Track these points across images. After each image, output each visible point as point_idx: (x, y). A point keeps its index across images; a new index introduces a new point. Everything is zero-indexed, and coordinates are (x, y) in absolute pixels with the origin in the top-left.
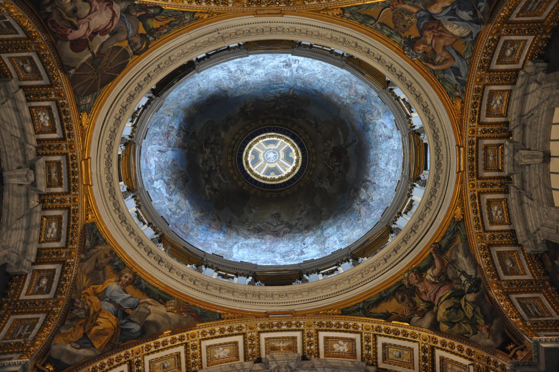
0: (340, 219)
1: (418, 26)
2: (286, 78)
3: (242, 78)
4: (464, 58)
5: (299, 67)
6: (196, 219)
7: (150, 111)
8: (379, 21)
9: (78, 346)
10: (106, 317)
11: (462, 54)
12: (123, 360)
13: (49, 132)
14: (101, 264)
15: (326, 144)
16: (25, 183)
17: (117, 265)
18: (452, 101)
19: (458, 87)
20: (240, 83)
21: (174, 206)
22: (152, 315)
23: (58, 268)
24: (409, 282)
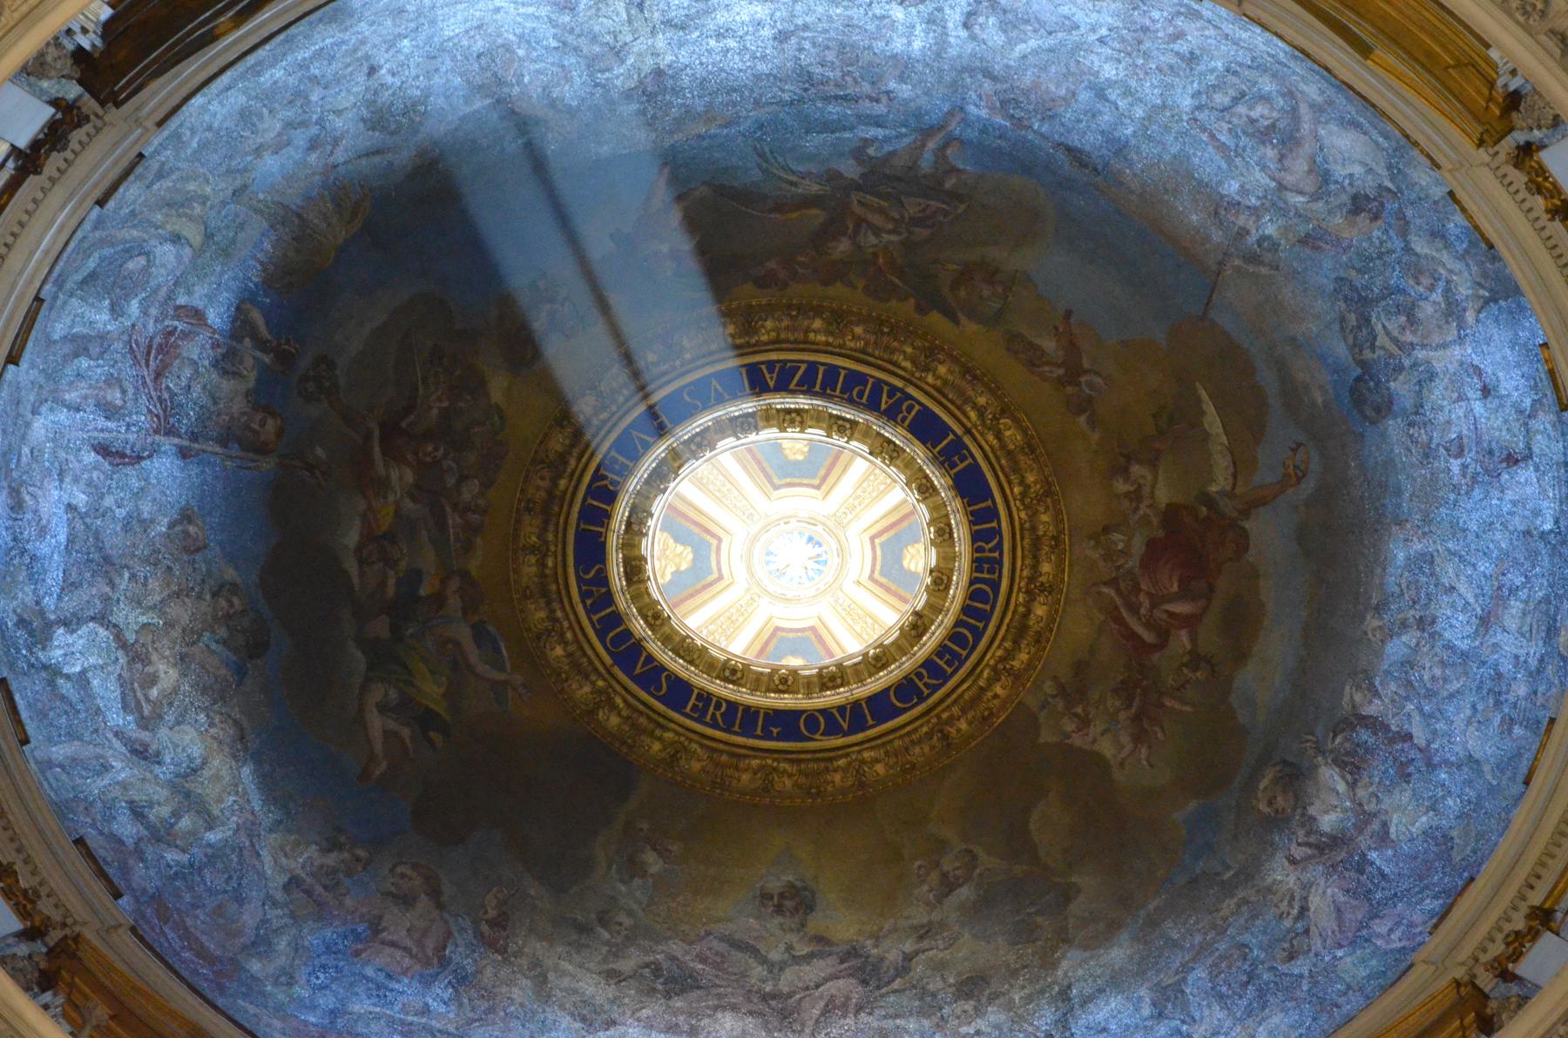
0: (1175, 944)
2: (904, 66)
6: (293, 883)
7: (58, 194)
15: (1121, 487)
21: (164, 793)
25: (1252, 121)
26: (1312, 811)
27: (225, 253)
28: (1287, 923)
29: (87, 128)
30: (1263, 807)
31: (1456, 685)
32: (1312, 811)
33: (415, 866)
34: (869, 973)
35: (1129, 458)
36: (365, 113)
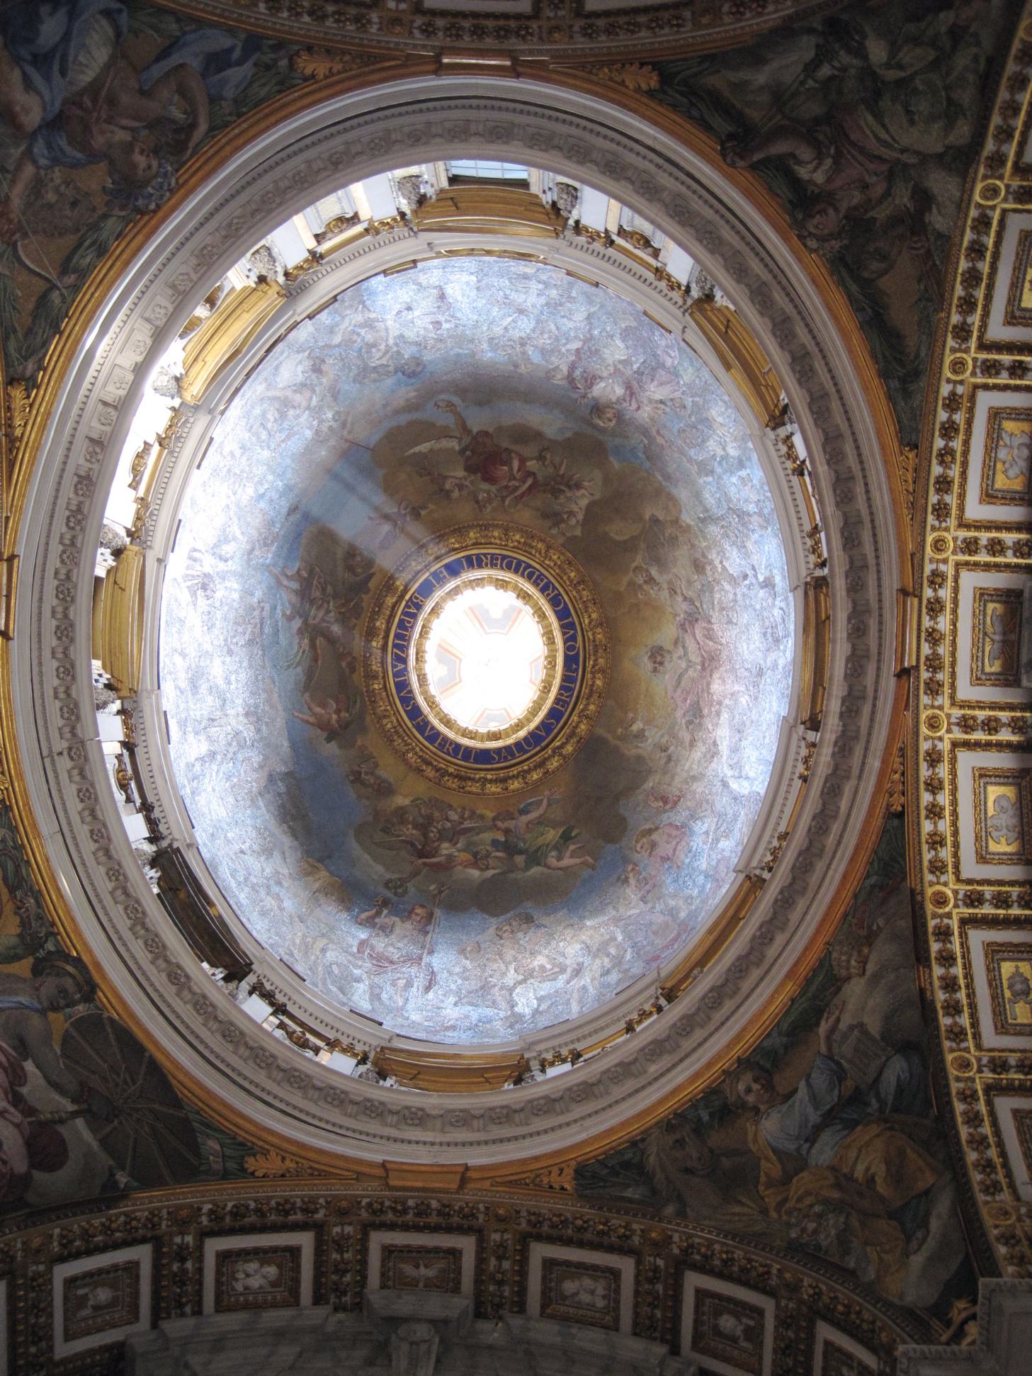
1: (75, 165)
2: (247, 592)
3: (233, 722)
4: (178, 39)
5: (215, 550)
6: (643, 899)
7: (295, 997)
8: (53, 277)
9: (919, 1234)
10: (853, 1154)
11: (167, 43)
12: (982, 1107)
13: (297, 1269)
14: (700, 1159)
15: (456, 494)
16: (435, 1348)
17: (711, 1115)
18: (306, 79)
19: (268, 57)
20: (249, 733)
21: (598, 961)
22: (866, 1020)
23: (693, 1281)
24: (832, 236)
25: (276, 420)
26: (614, 399)
27: (332, 929)
28: (668, 410)
29: (264, 981)
30: (612, 424)
31: (553, 327)
32: (614, 399)
33: (637, 842)
34: (692, 619)
35: (442, 490)
36: (262, 859)
